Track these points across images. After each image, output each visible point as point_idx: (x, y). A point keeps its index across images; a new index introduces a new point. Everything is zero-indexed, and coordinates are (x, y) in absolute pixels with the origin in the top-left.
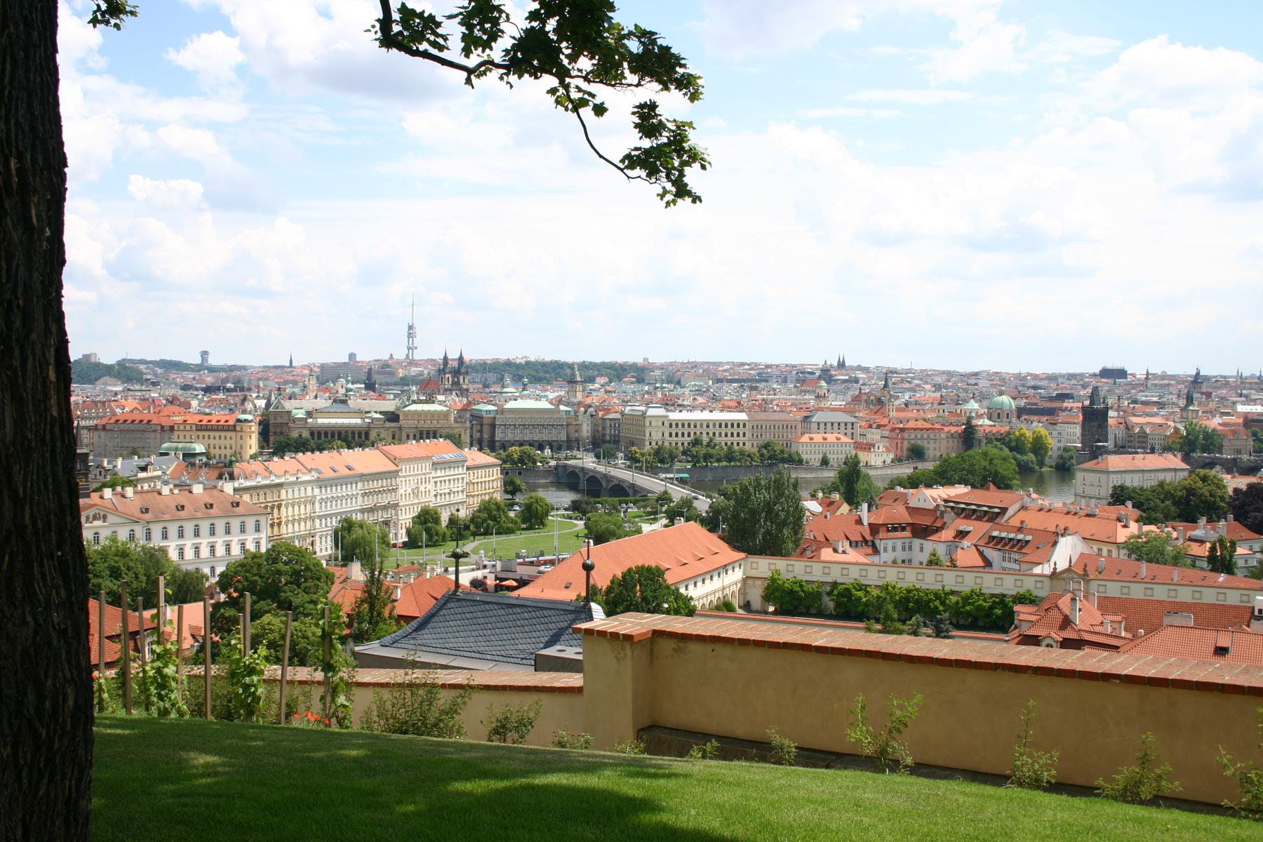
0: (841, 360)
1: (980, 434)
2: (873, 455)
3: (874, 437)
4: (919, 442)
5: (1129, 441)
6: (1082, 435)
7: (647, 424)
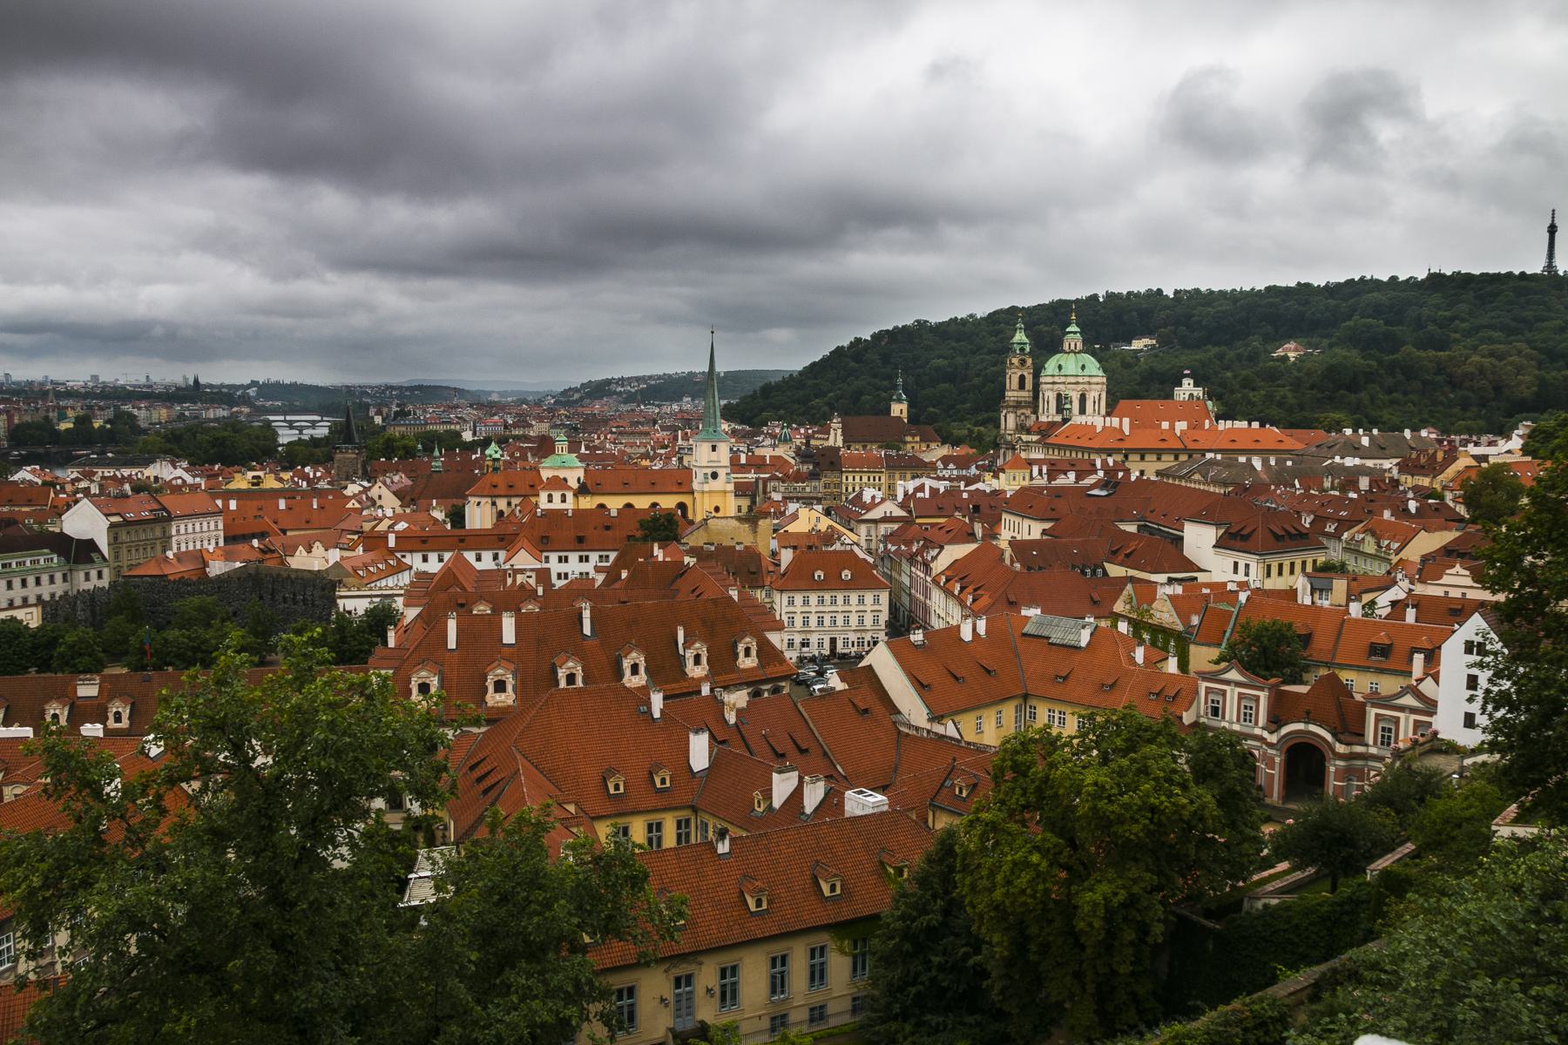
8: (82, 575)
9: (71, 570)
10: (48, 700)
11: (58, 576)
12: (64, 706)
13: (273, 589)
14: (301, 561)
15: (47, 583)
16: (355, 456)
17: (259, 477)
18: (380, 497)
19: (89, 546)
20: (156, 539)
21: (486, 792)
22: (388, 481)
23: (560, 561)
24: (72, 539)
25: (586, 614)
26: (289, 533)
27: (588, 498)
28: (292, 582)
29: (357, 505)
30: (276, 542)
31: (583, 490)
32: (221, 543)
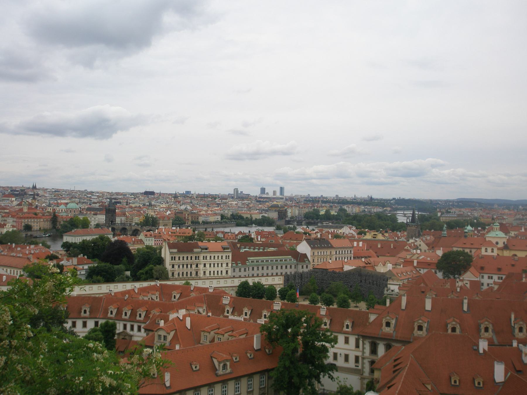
0: (34, 185)
1: (59, 219)
3: (10, 221)
4: (30, 223)
5: (127, 221)
6: (106, 219)
8: (301, 266)
9: (297, 264)
10: (263, 309)
11: (293, 266)
12: (268, 312)
13: (366, 279)
14: (381, 269)
15: (289, 268)
16: (415, 228)
17: (376, 235)
18: (420, 245)
19: (305, 256)
20: (328, 255)
21: (394, 372)
22: (424, 239)
23: (489, 278)
24: (300, 253)
25: (466, 301)
26: (379, 257)
27: (508, 252)
28: (373, 276)
29: (409, 248)
30: (372, 260)
31: (506, 247)
32: (352, 258)
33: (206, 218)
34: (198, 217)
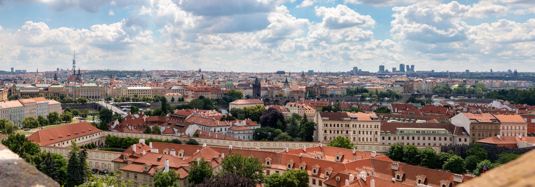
2: (188, 99)
4: (202, 95)
7: (122, 90)
33: (333, 91)
34: (326, 91)
